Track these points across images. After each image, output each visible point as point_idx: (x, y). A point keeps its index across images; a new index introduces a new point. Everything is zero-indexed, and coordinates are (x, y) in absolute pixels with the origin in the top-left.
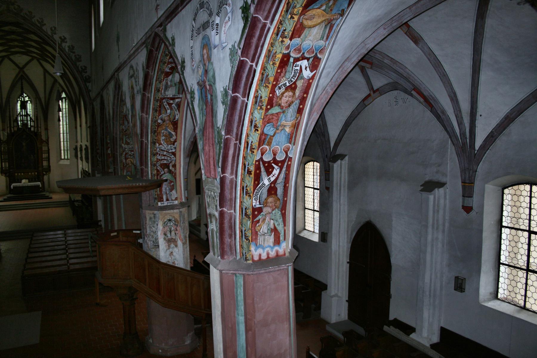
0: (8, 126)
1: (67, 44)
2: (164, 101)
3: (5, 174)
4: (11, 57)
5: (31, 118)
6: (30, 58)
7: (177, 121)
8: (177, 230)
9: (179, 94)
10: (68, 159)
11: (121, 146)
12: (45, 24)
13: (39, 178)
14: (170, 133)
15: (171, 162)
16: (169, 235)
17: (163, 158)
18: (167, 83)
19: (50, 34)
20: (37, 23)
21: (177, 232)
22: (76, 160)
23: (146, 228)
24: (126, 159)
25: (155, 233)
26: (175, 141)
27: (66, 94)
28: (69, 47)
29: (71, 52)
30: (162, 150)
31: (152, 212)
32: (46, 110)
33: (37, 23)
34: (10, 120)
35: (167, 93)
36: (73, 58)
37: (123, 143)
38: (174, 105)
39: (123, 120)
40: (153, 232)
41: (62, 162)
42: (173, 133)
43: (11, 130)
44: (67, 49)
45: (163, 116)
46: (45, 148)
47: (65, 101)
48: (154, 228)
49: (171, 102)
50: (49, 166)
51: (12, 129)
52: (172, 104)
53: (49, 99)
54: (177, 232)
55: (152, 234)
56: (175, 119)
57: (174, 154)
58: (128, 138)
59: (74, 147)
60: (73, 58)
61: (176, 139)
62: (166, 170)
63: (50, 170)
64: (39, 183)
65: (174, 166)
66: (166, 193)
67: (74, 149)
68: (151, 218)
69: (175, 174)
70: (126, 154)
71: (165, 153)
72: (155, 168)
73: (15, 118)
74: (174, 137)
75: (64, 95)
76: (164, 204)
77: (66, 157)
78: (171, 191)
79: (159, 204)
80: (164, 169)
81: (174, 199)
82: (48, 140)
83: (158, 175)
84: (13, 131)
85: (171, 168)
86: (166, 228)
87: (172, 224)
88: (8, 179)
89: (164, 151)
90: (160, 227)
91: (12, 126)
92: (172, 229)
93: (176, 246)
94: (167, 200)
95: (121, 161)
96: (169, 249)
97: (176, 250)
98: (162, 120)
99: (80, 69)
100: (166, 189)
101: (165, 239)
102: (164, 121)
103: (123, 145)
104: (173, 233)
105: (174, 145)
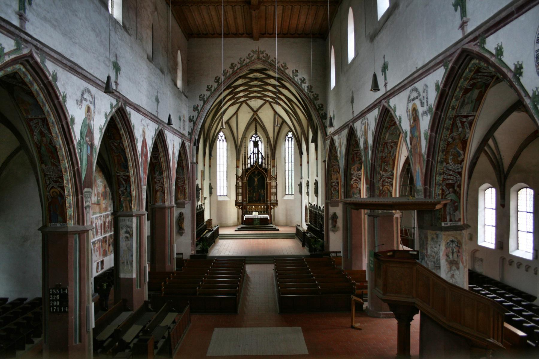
1: (306, 85)
2: (458, 119)
3: (239, 206)
4: (248, 102)
5: (262, 156)
6: (263, 102)
7: (467, 139)
8: (459, 252)
9: (473, 111)
10: (292, 194)
11: (379, 173)
12: (288, 68)
13: (267, 211)
14: (458, 152)
15: (456, 182)
16: (451, 257)
17: (449, 177)
18: (464, 101)
19: (292, 76)
20: (281, 67)
21: (459, 254)
23: (427, 249)
24: (383, 186)
25: (437, 253)
26: (463, 160)
27: (293, 134)
28: (308, 87)
29: (310, 92)
30: (449, 170)
31: (434, 232)
32: (273, 148)
33: (281, 67)
34: (245, 157)
35: (462, 110)
36: (312, 97)
37: (381, 170)
38: (466, 123)
39: (384, 148)
40: (434, 252)
41: (286, 197)
42: (462, 152)
43: (245, 167)
44: (306, 89)
45: (454, 134)
46: (273, 184)
47: (292, 140)
48: (436, 249)
49: (465, 120)
50: (277, 200)
52: (465, 122)
54: (459, 254)
55: (433, 254)
56: (465, 137)
57: (460, 174)
58: (387, 165)
59: (299, 183)
60: (312, 97)
61: (464, 158)
62: (451, 190)
63: (277, 204)
64: (267, 216)
65: (459, 186)
66: (450, 213)
68: (433, 239)
69: (460, 194)
70: (383, 181)
71: (451, 173)
72: (441, 187)
74: (462, 157)
75: (290, 135)
76: (447, 224)
77: (290, 193)
78: (455, 212)
79: (443, 224)
80: (449, 190)
81: (457, 220)
82: (276, 176)
83: (443, 194)
85: (456, 188)
86: (448, 249)
87: (454, 245)
88: (240, 211)
89: (451, 170)
90: (443, 247)
92: (455, 250)
93: (458, 269)
94: (451, 220)
95: (378, 188)
96: (450, 271)
97: (457, 272)
98: (452, 138)
99: (317, 107)
100: (450, 210)
101: (447, 260)
102: (454, 139)
103: (381, 172)
104: (455, 255)
105: (461, 164)
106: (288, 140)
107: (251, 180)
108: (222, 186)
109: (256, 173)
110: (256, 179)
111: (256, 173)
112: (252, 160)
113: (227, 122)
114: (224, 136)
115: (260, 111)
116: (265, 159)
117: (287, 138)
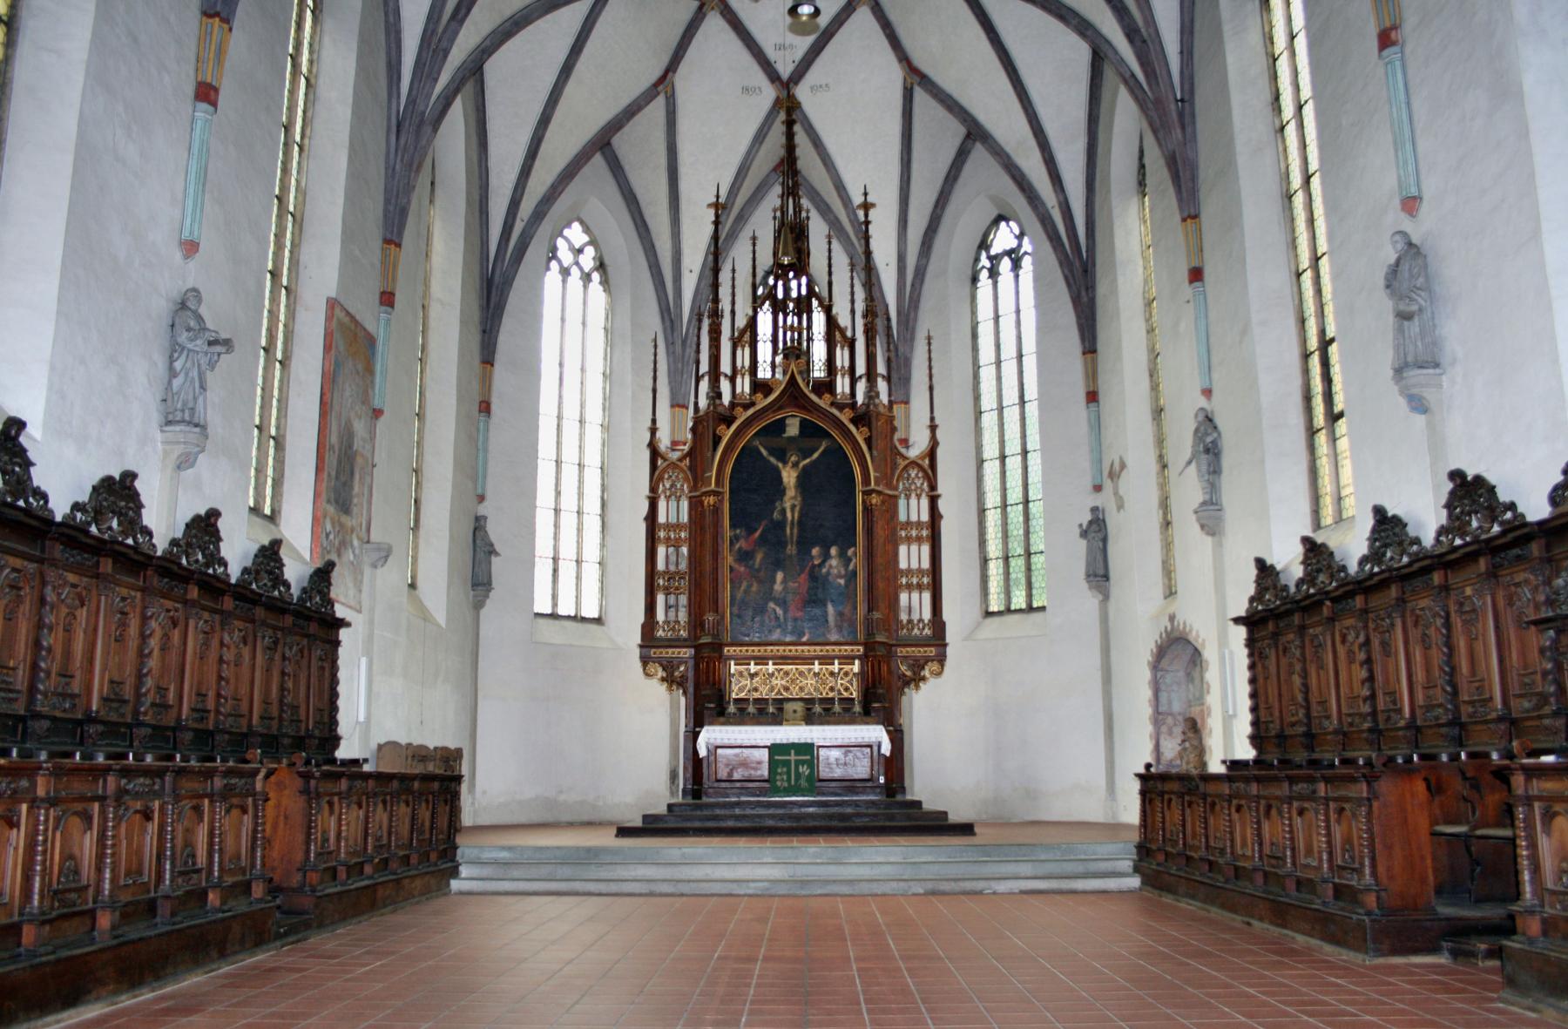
0: (704, 367)
5: (831, 323)
22: (1091, 601)
43: (716, 394)
46: (914, 509)
47: (1016, 265)
51: (725, 386)
53: (920, 273)
59: (1086, 517)
67: (1084, 534)
73: (741, 322)
77: (1019, 601)
82: (932, 454)
84: (726, 399)
91: (726, 367)
106: (994, 273)
107: (753, 485)
108: (568, 551)
109: (793, 429)
110: (789, 476)
111: (793, 429)
112: (764, 351)
113: (602, 144)
114: (590, 252)
115: (814, 76)
116: (852, 344)
117: (984, 262)
